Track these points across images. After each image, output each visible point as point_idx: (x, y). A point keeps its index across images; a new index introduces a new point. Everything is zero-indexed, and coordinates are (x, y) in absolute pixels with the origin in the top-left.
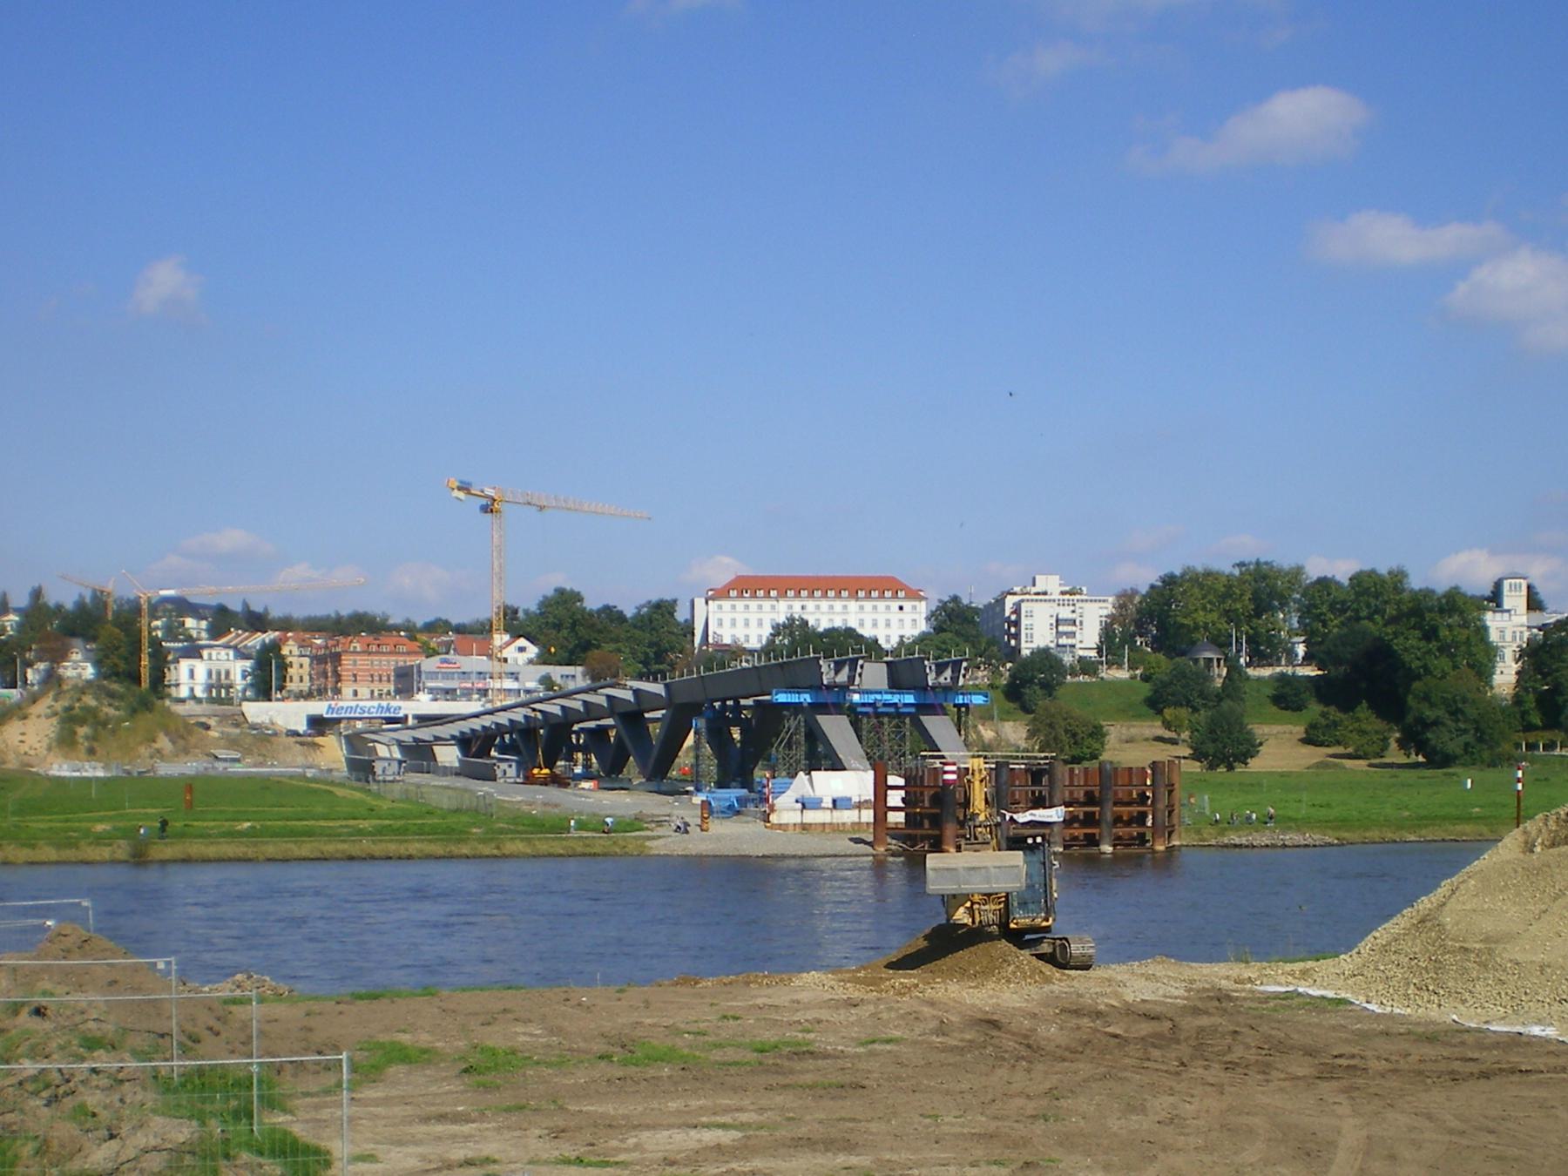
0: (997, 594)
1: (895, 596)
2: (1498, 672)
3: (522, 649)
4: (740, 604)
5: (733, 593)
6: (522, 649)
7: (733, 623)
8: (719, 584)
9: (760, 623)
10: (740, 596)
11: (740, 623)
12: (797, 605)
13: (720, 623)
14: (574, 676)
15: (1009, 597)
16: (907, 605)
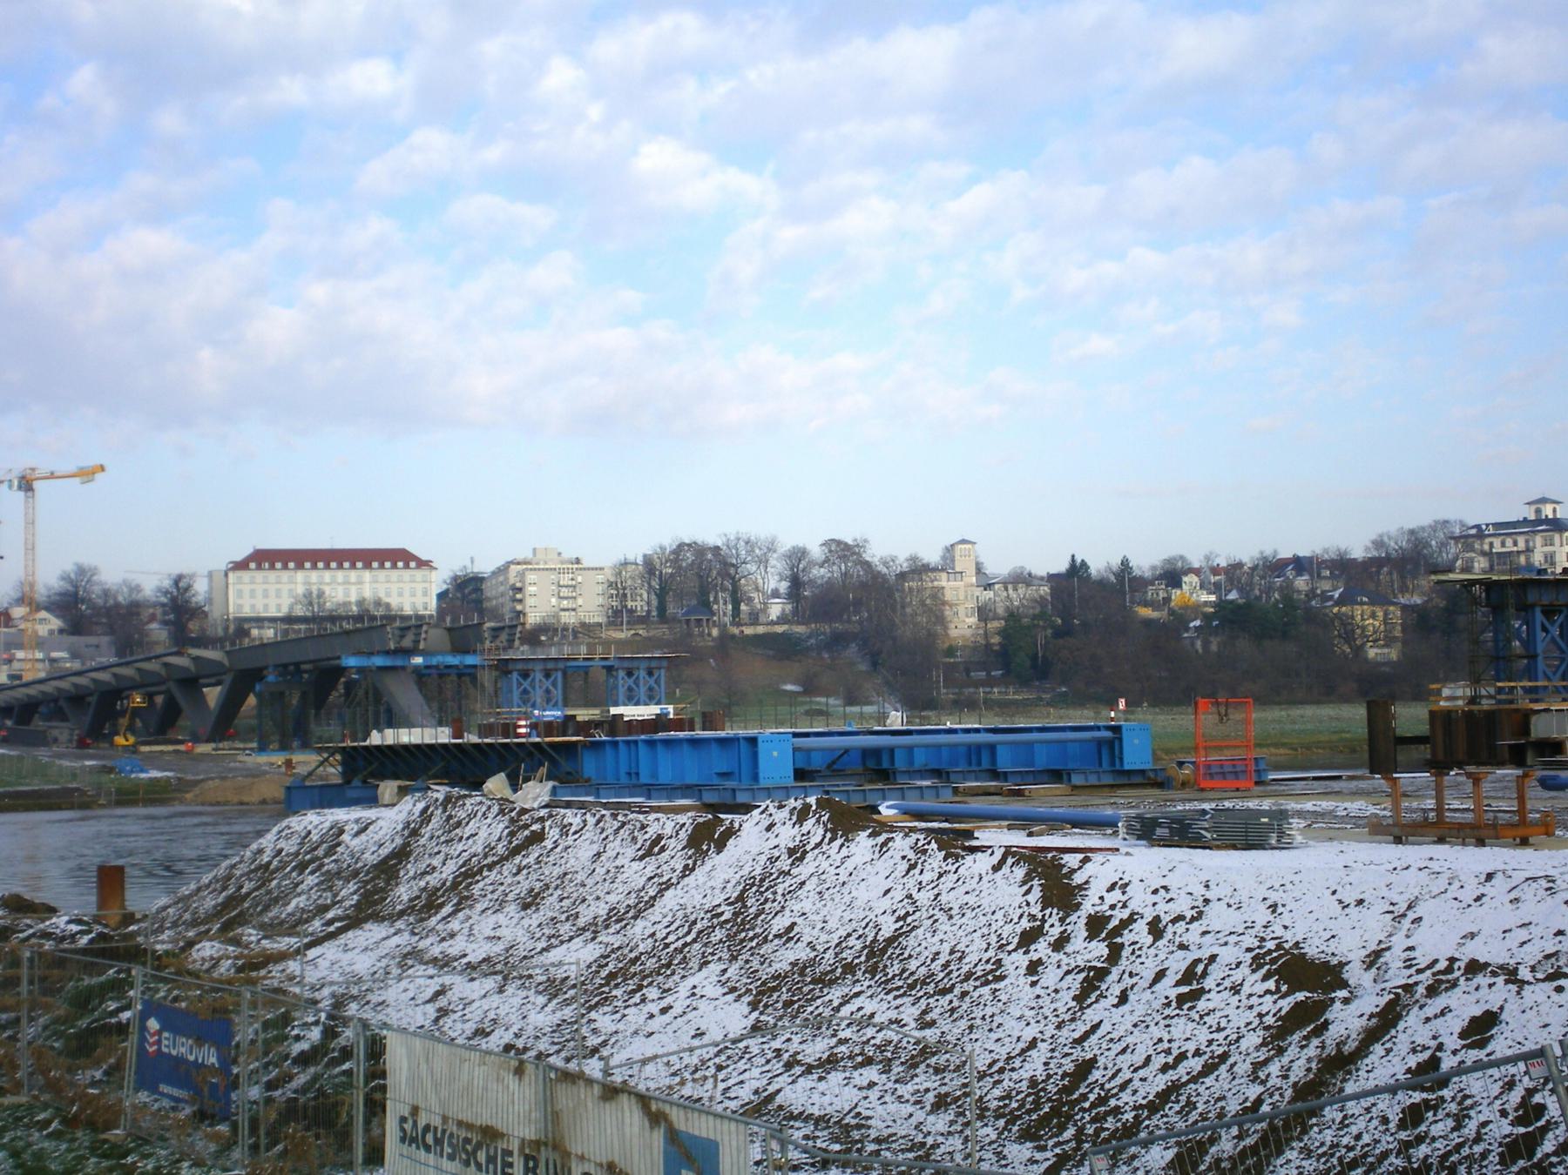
0: (500, 563)
1: (407, 566)
2: (953, 626)
3: (43, 620)
4: (259, 575)
5: (253, 565)
6: (43, 620)
7: (253, 594)
8: (239, 557)
9: (278, 594)
10: (259, 568)
11: (259, 593)
12: (314, 576)
13: (240, 594)
14: (97, 646)
15: (512, 567)
16: (419, 574)
